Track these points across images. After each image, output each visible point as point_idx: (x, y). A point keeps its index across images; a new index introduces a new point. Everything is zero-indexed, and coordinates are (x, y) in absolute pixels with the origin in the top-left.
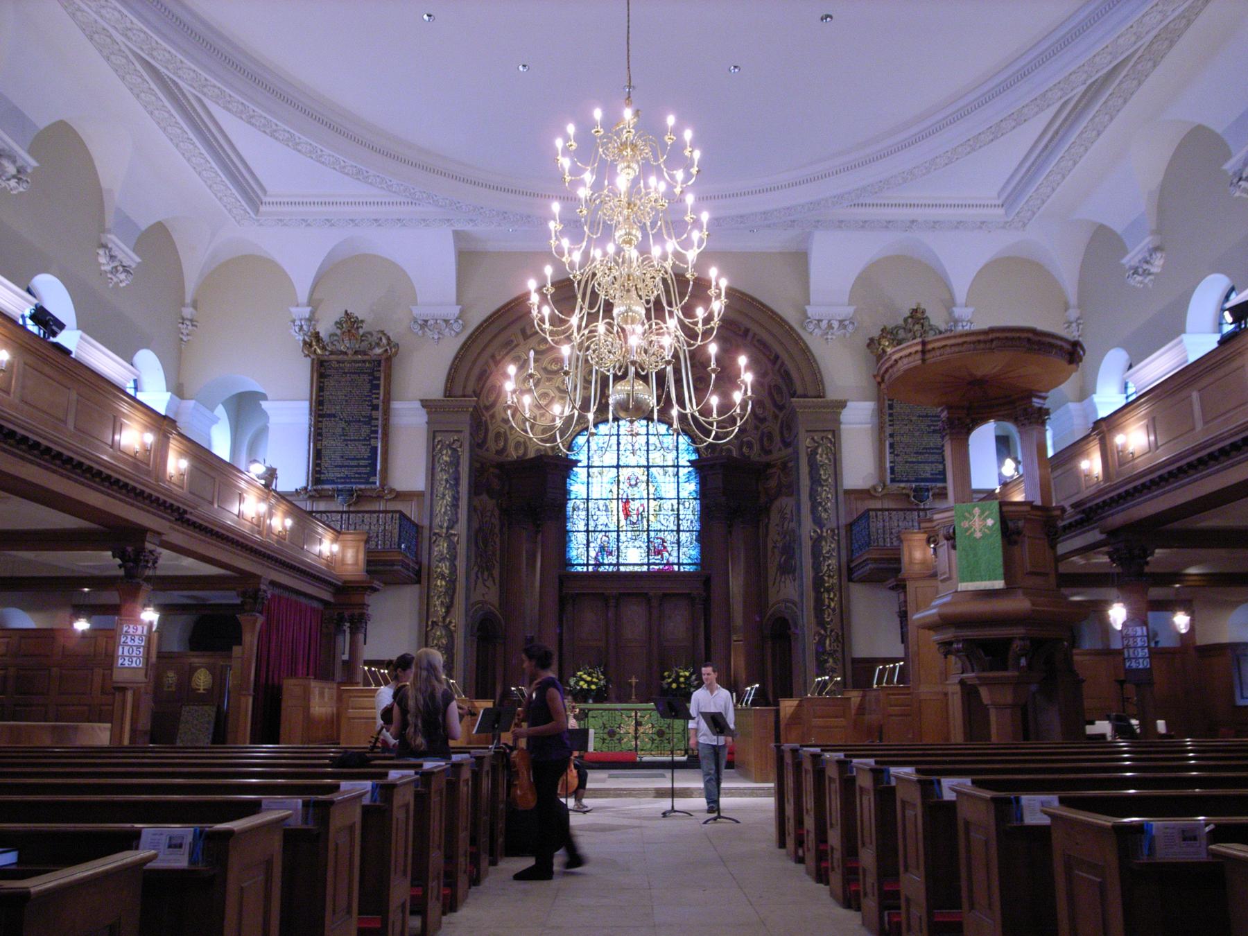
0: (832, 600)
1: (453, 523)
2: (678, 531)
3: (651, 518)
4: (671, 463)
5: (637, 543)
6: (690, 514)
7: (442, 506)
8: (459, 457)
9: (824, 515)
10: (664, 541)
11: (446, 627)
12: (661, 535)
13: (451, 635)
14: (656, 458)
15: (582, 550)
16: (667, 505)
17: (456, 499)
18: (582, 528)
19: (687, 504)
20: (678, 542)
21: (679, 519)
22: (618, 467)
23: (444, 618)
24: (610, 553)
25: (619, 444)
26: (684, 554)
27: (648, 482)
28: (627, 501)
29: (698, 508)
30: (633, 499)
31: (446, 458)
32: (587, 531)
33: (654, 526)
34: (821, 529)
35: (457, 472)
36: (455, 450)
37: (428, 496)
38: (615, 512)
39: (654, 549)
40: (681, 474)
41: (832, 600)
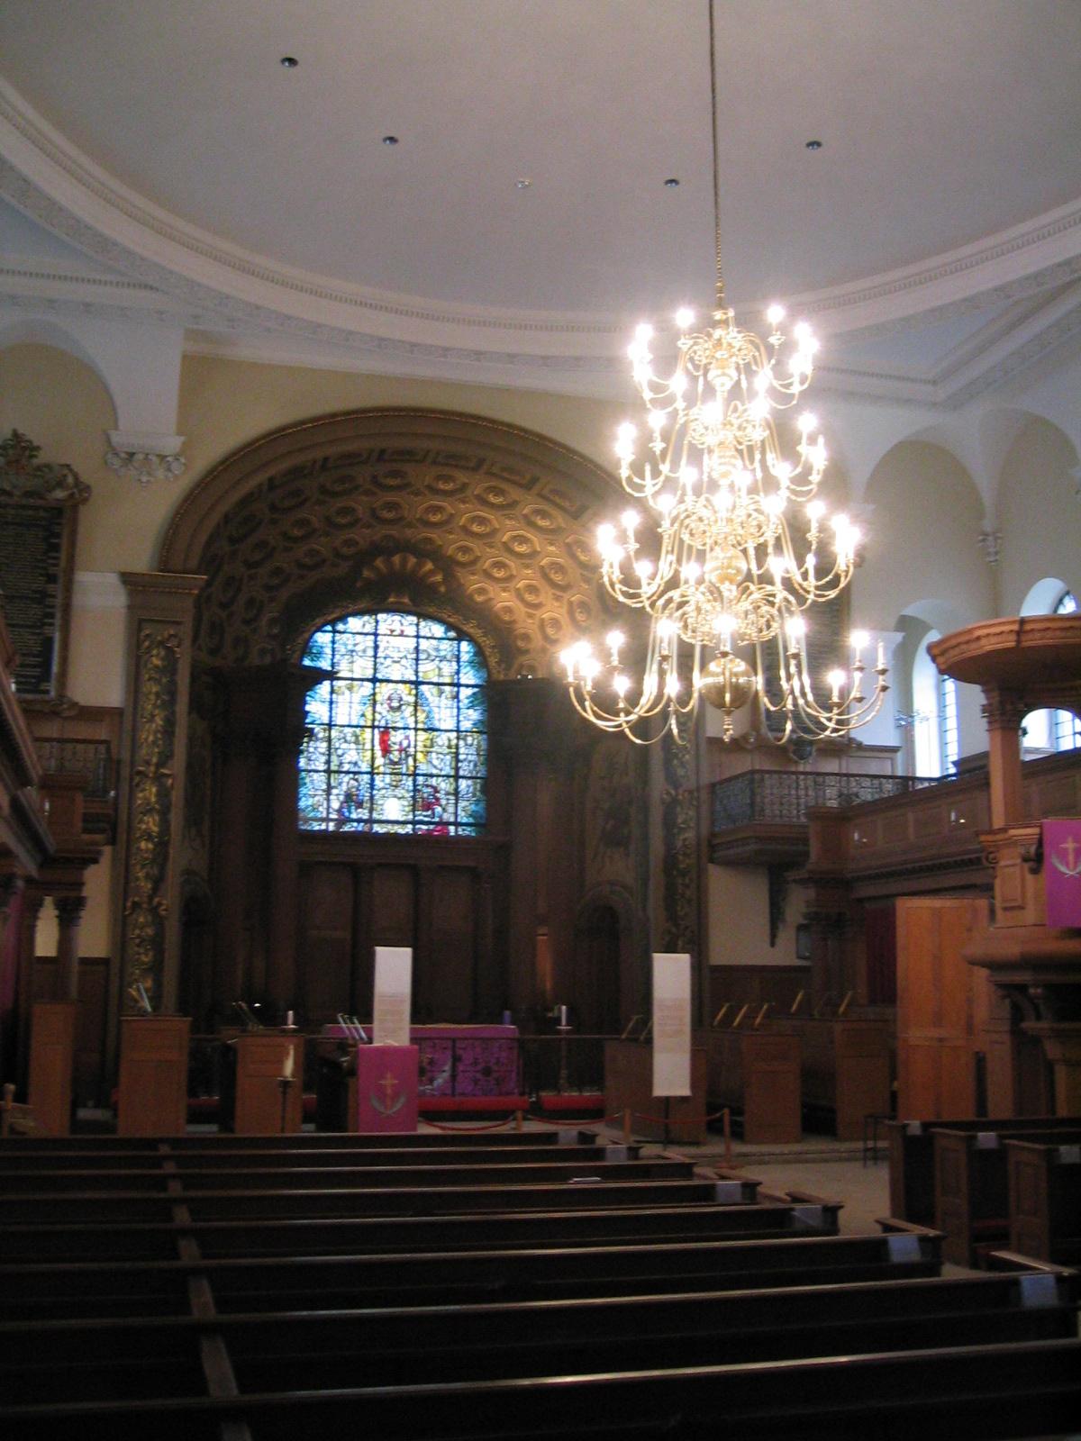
0: (687, 886)
1: (166, 758)
3: (420, 756)
4: (447, 680)
5: (399, 792)
6: (470, 753)
7: (150, 733)
8: (176, 661)
9: (681, 772)
10: (436, 790)
11: (154, 910)
12: (434, 781)
13: (159, 922)
14: (428, 670)
15: (321, 798)
16: (442, 739)
17: (170, 723)
18: (322, 767)
19: (470, 740)
20: (456, 793)
21: (458, 761)
22: (374, 680)
23: (151, 898)
24: (360, 805)
25: (376, 647)
26: (459, 811)
27: (416, 705)
28: (386, 731)
29: (484, 745)
30: (395, 729)
31: (156, 661)
32: (328, 772)
33: (423, 768)
34: (676, 788)
35: (173, 682)
36: (170, 651)
37: (128, 718)
38: (368, 746)
39: (422, 801)
40: (462, 696)
41: (687, 886)
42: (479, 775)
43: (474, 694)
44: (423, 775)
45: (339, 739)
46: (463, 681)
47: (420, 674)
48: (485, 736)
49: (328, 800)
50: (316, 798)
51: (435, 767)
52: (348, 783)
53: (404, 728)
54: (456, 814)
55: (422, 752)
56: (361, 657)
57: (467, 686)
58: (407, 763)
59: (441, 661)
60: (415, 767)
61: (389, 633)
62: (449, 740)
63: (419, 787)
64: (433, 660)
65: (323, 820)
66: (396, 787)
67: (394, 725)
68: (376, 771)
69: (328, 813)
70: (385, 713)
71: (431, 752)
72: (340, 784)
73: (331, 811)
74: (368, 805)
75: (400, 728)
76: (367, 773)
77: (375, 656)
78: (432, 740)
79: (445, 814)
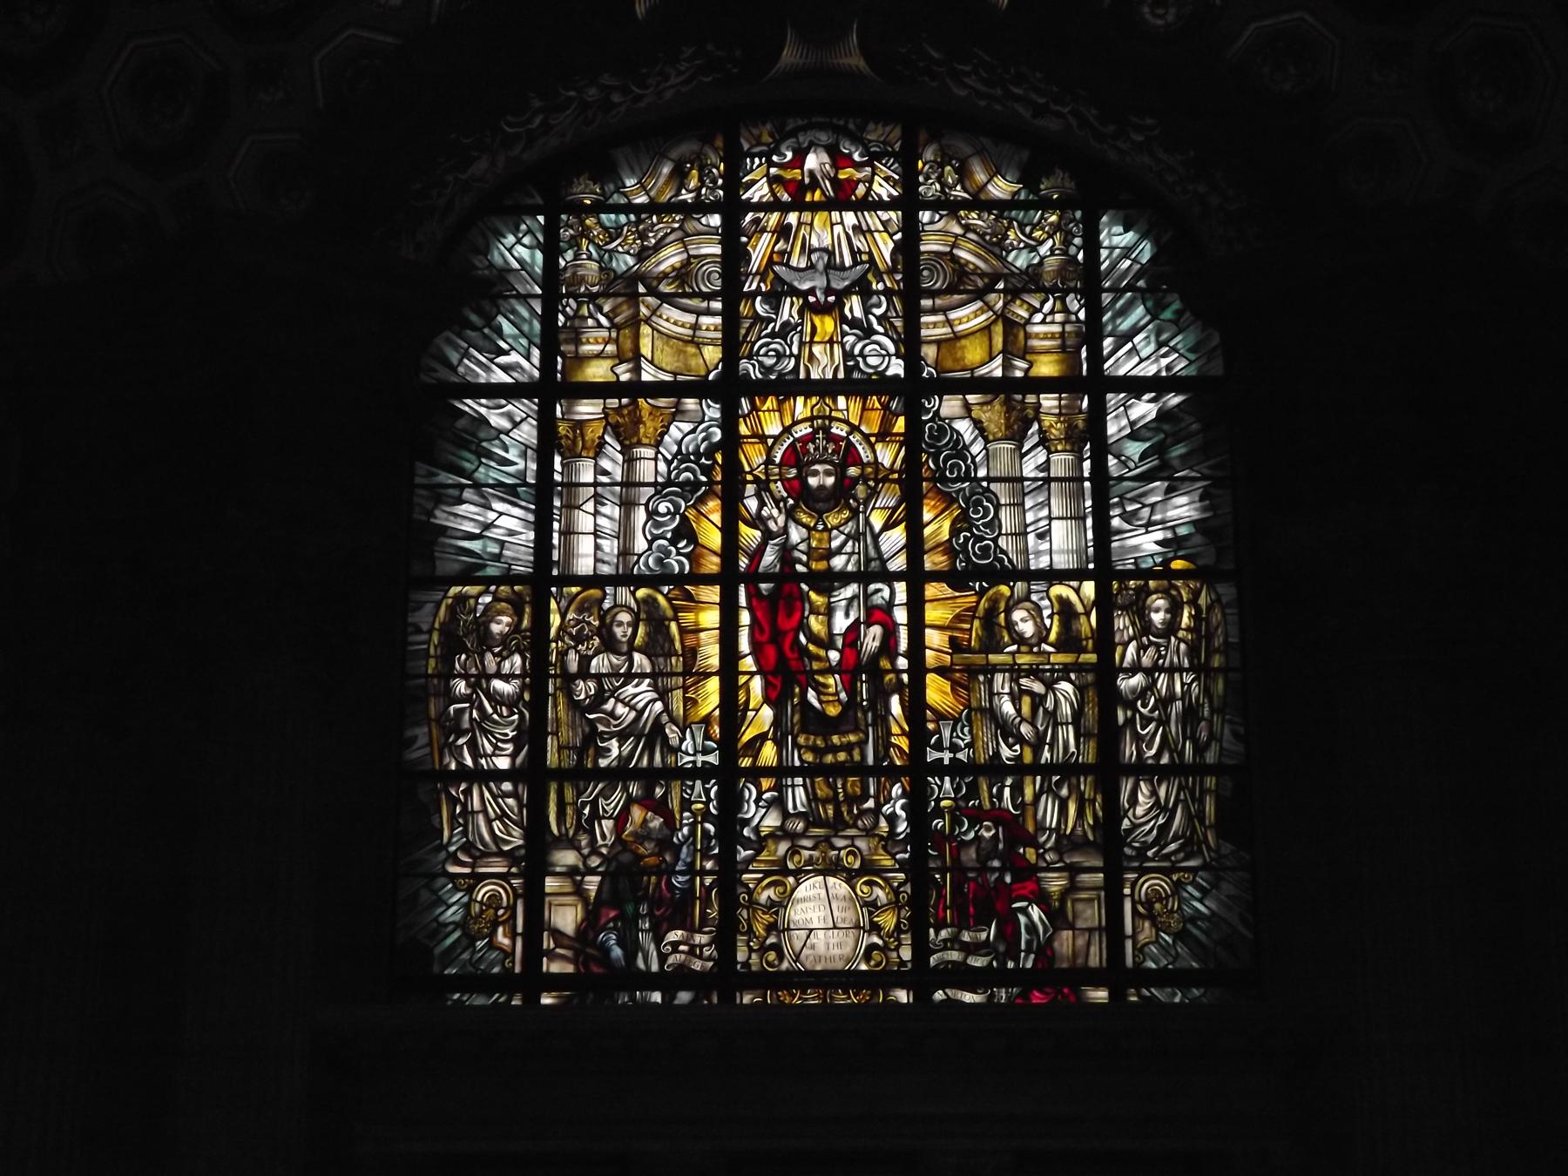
2: (1108, 771)
3: (937, 692)
4: (1047, 367)
5: (850, 846)
10: (1016, 829)
20: (1109, 838)
22: (729, 389)
24: (677, 912)
25: (734, 256)
30: (828, 581)
38: (711, 655)
42: (1210, 757)
43: (1163, 415)
44: (956, 769)
45: (579, 639)
46: (1123, 365)
47: (929, 352)
48: (1227, 591)
49: (535, 899)
50: (482, 892)
51: (1006, 730)
52: (621, 820)
53: (862, 578)
54: (1113, 930)
55: (942, 671)
56: (666, 298)
57: (1135, 387)
58: (883, 718)
59: (1013, 294)
60: (919, 736)
61: (786, 197)
62: (1066, 610)
63: (938, 823)
64: (979, 294)
65: (507, 982)
66: (837, 825)
67: (818, 566)
68: (746, 762)
69: (534, 953)
70: (776, 519)
71: (991, 670)
72: (587, 826)
73: (548, 942)
74: (713, 913)
75: (845, 578)
76: (704, 773)
77: (732, 293)
78: (989, 619)
79: (1067, 935)
